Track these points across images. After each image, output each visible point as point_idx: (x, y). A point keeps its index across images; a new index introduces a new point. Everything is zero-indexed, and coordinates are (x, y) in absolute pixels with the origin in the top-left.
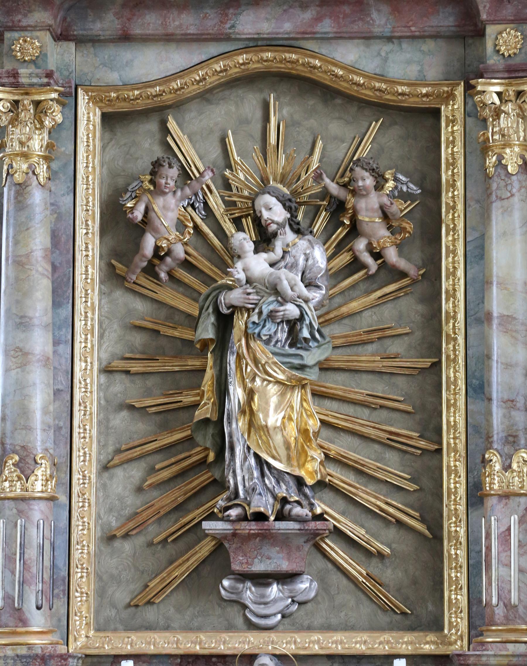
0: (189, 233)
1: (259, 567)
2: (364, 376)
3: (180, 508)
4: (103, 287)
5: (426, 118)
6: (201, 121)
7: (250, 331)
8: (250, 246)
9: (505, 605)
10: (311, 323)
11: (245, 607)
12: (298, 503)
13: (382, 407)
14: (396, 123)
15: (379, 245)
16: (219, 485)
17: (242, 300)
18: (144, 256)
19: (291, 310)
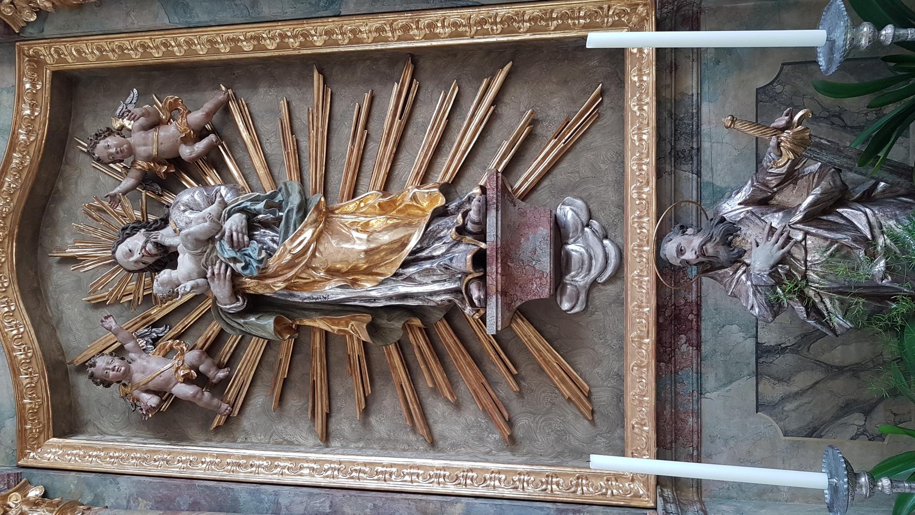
0: (179, 344)
1: (545, 264)
2: (333, 149)
3: (478, 360)
4: (239, 440)
5: (70, 88)
6: (77, 330)
7: (255, 274)
8: (165, 275)
10: (251, 200)
11: (594, 283)
12: (465, 215)
13: (366, 127)
14: (82, 124)
15: (185, 130)
16: (451, 313)
17: (222, 282)
18: (194, 396)
19: (235, 223)
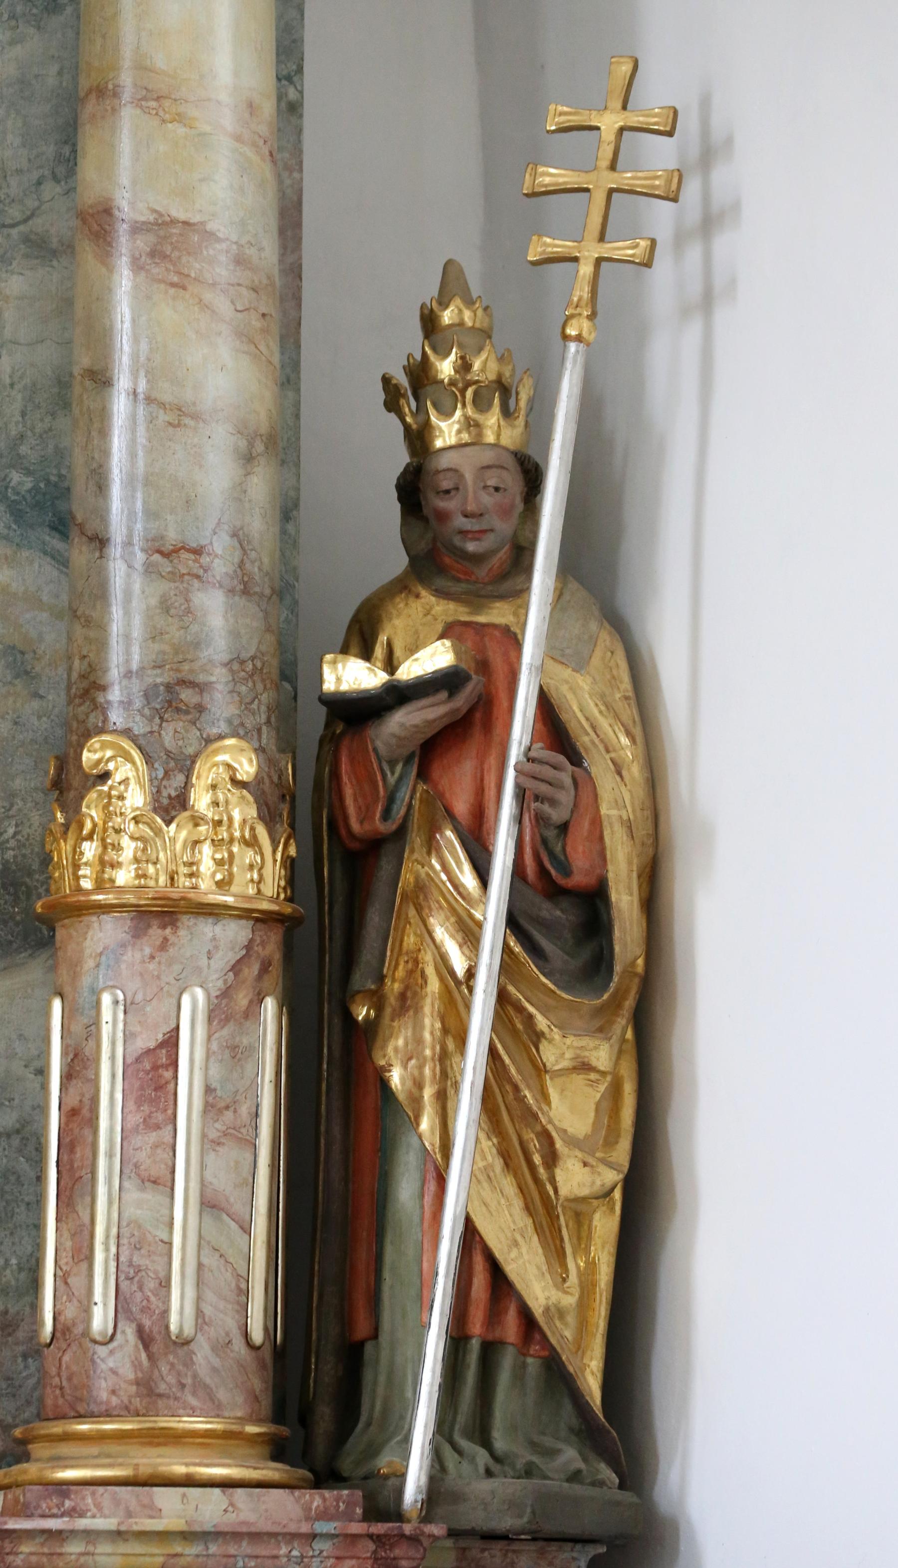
9: (145, 1339)
